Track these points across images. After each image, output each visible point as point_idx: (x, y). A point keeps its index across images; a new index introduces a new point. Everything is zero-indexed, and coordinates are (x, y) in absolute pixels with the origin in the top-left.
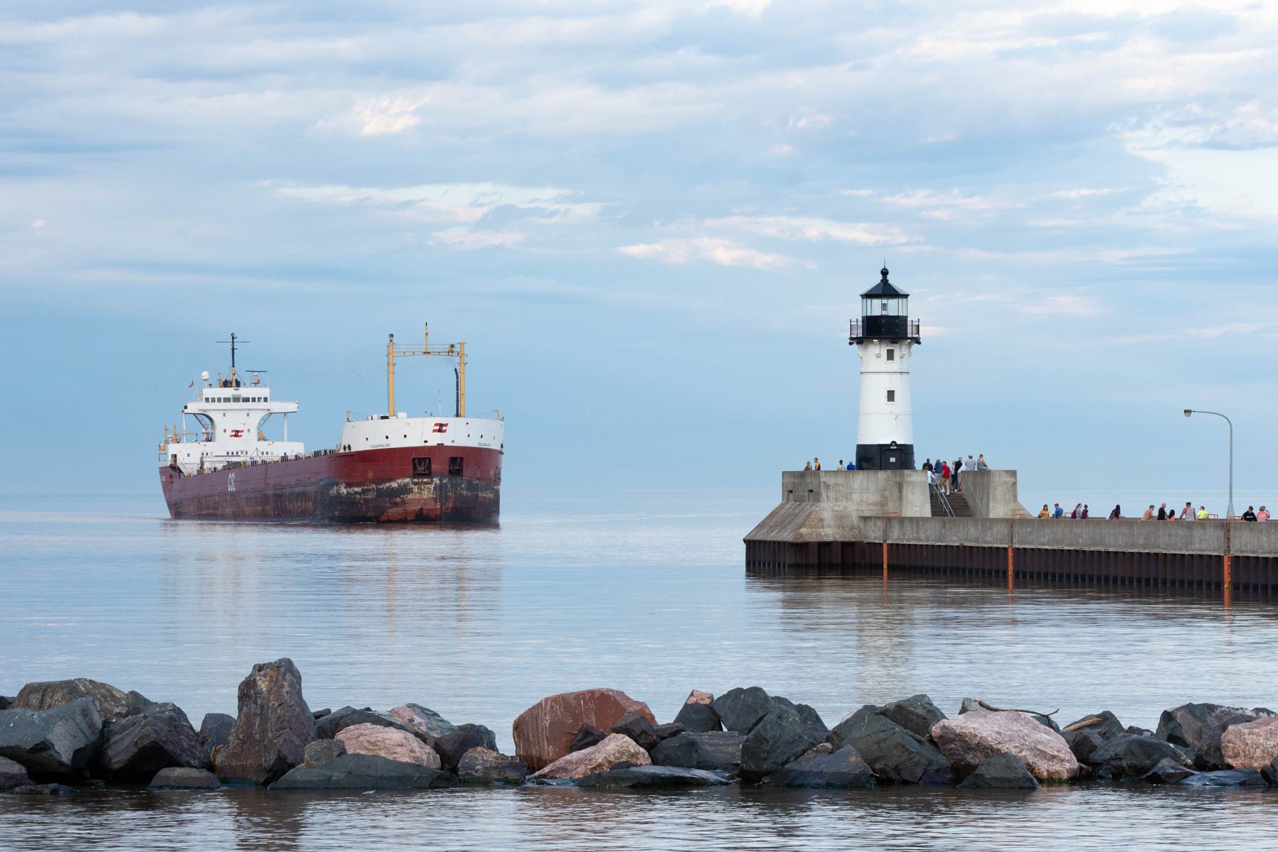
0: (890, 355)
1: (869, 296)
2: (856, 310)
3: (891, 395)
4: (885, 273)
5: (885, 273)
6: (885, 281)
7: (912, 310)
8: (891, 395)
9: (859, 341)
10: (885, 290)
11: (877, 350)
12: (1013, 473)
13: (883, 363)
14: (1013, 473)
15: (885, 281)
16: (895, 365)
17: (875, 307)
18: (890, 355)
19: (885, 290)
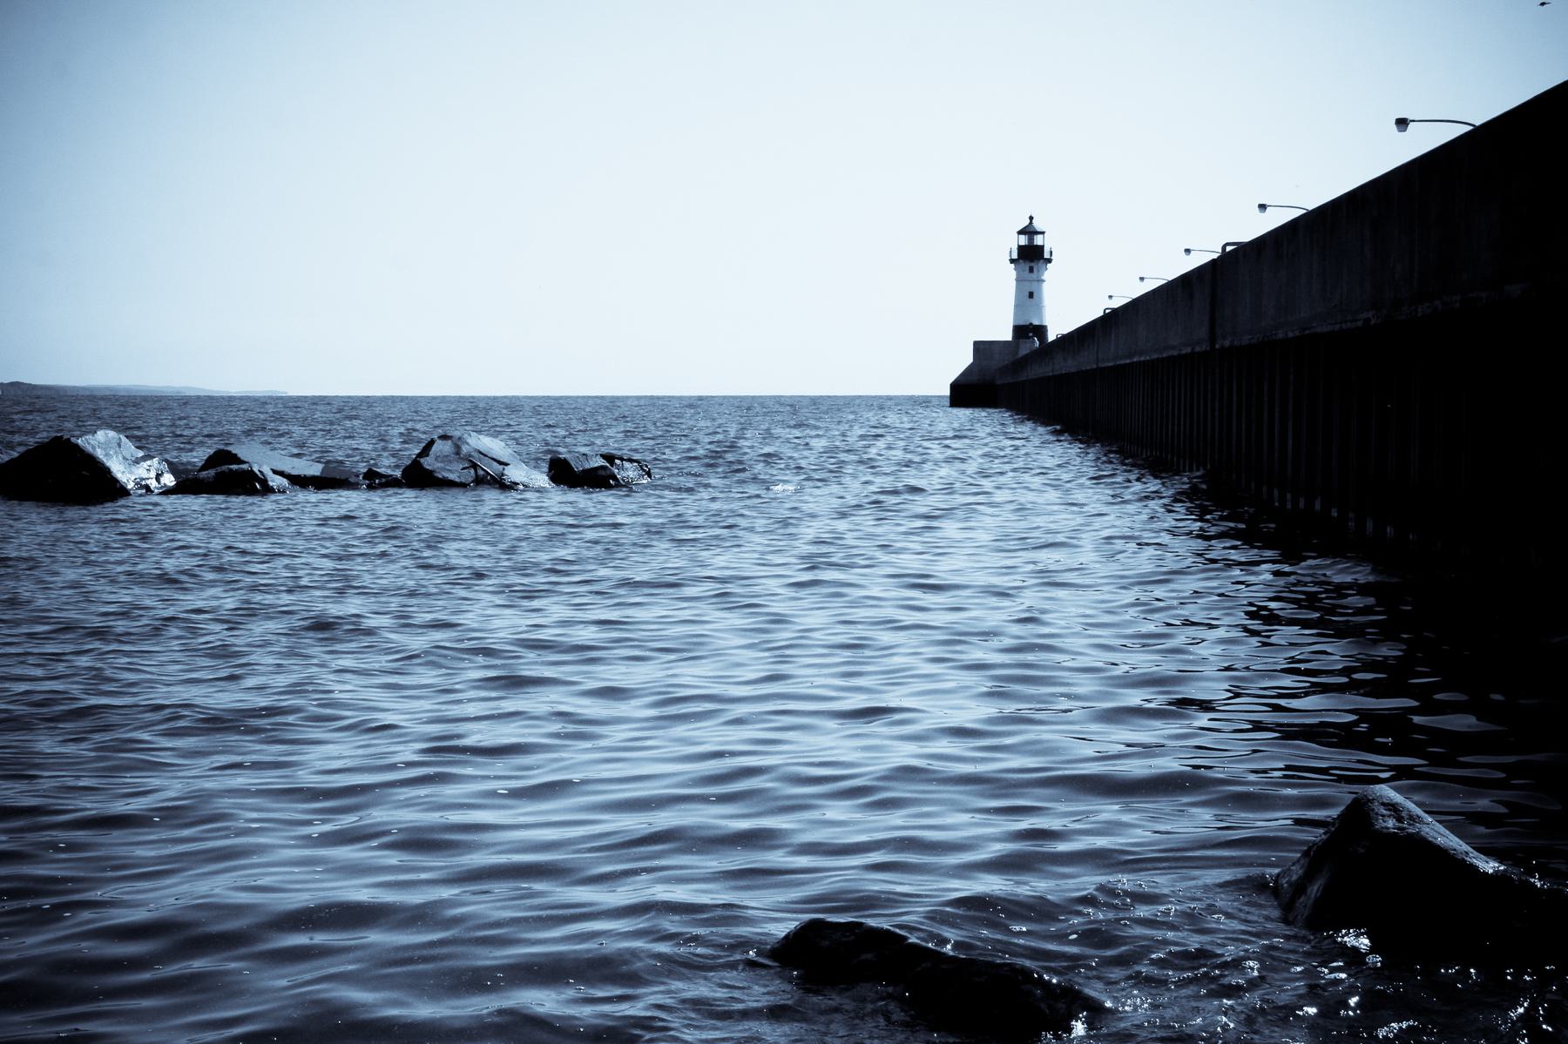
0: (1031, 270)
1: (1020, 233)
2: (1016, 242)
4: (1031, 218)
5: (1031, 218)
7: (1046, 241)
9: (1012, 261)
10: (1029, 231)
11: (1026, 266)
17: (1023, 240)
18: (1031, 270)
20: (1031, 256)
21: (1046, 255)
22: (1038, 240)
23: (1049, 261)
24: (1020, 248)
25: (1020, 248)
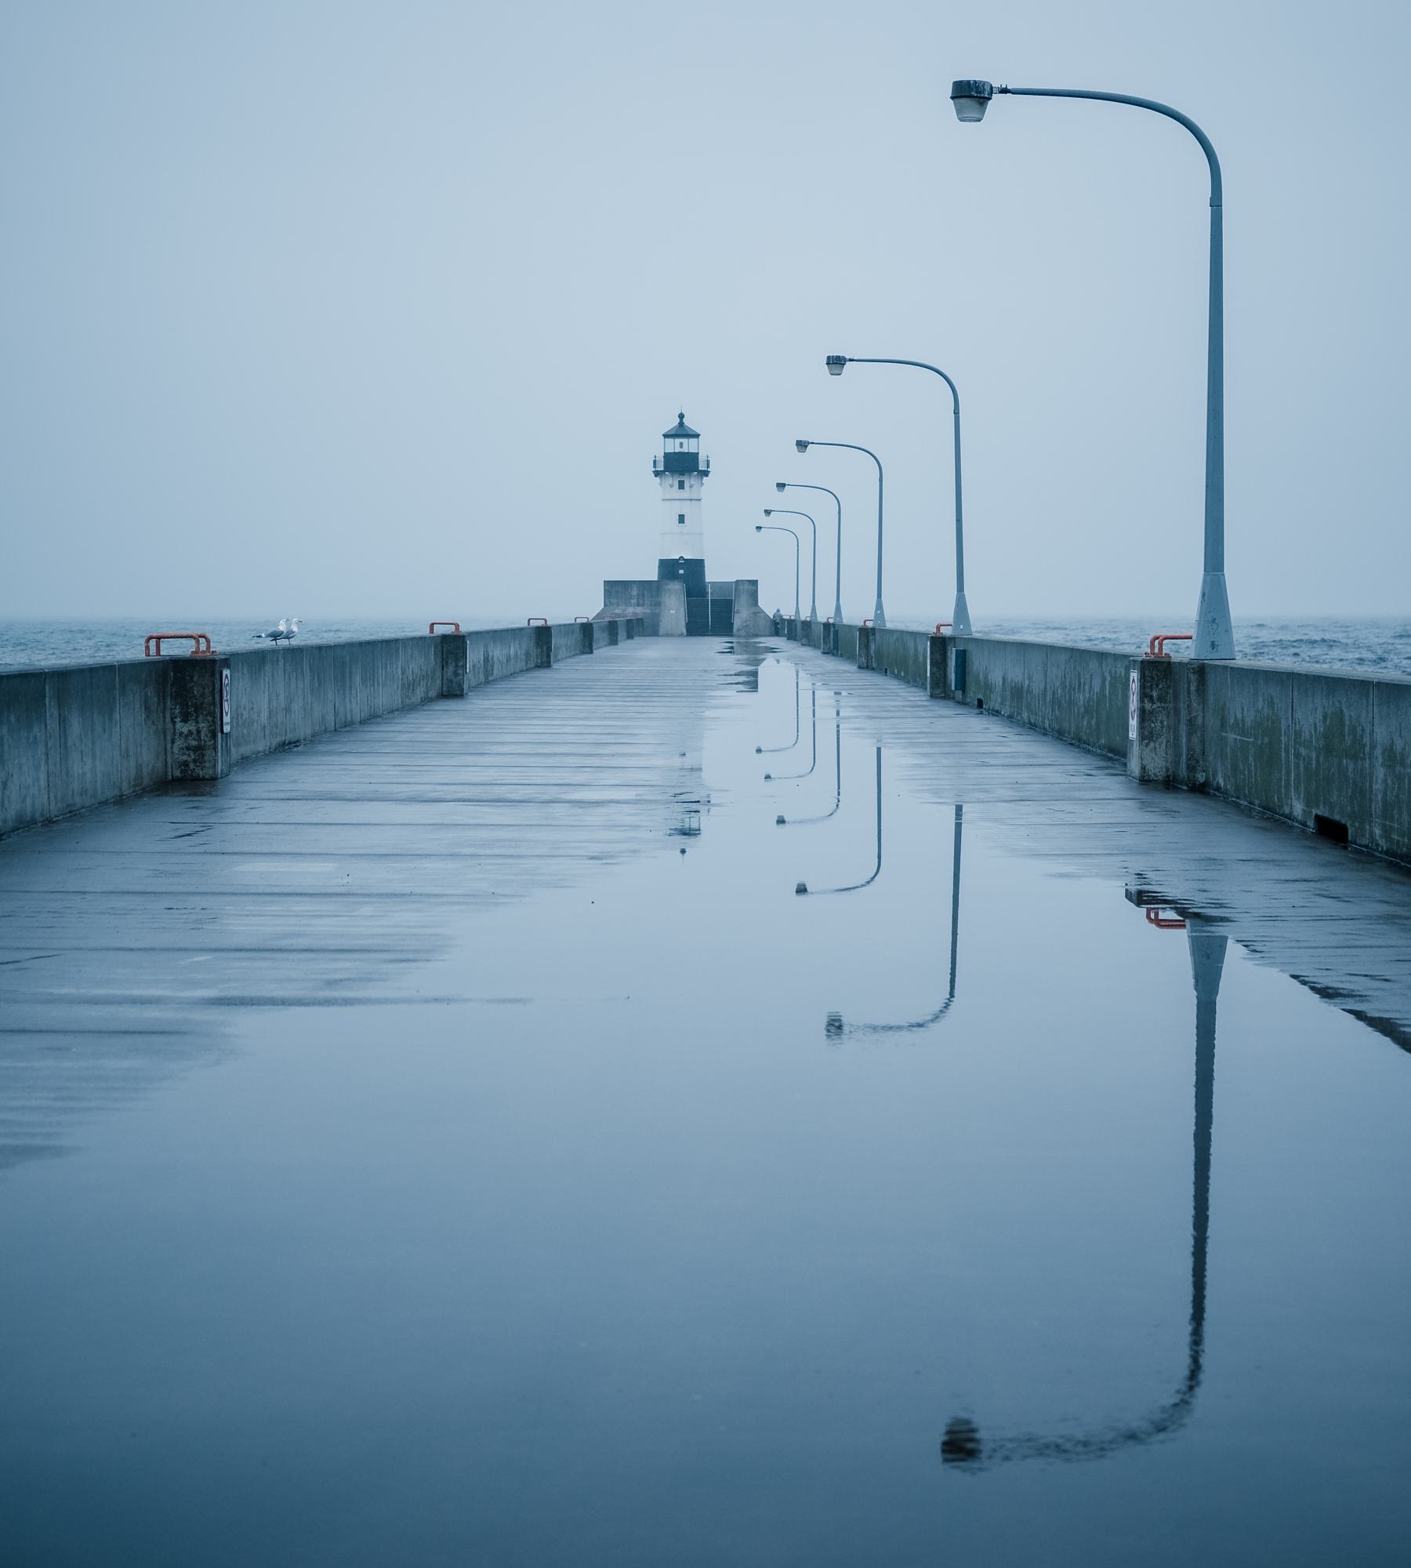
0: (681, 485)
1: (666, 436)
2: (660, 447)
3: (681, 519)
4: (681, 416)
5: (681, 416)
6: (681, 424)
7: (702, 448)
8: (681, 519)
9: (657, 474)
10: (681, 432)
11: (672, 481)
12: (754, 583)
13: (675, 492)
14: (754, 583)
15: (681, 424)
16: (685, 494)
17: (674, 446)
18: (681, 485)
19: (681, 432)
20: (682, 466)
21: (702, 467)
22: (689, 446)
23: (706, 473)
24: (667, 456)
25: (667, 456)
